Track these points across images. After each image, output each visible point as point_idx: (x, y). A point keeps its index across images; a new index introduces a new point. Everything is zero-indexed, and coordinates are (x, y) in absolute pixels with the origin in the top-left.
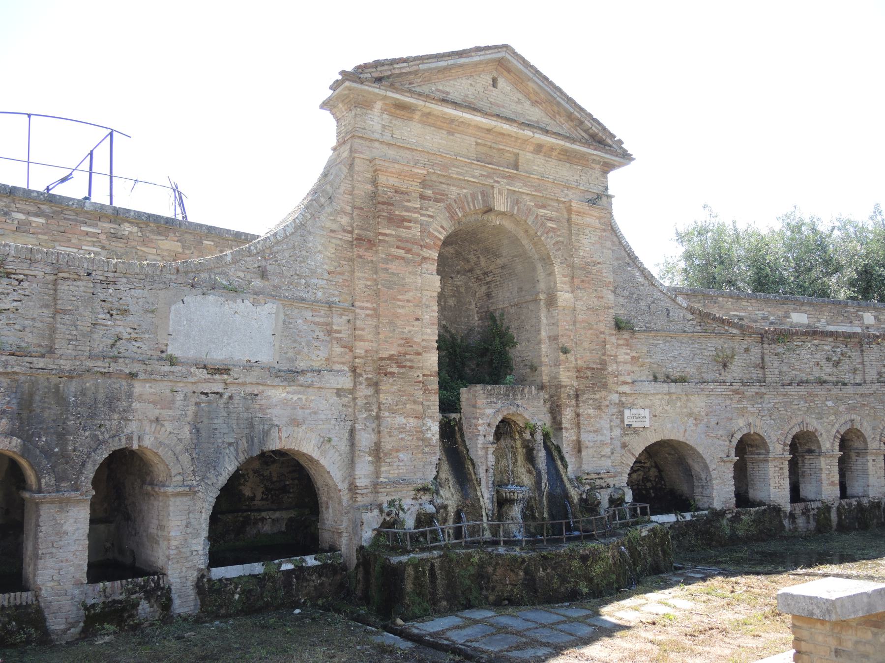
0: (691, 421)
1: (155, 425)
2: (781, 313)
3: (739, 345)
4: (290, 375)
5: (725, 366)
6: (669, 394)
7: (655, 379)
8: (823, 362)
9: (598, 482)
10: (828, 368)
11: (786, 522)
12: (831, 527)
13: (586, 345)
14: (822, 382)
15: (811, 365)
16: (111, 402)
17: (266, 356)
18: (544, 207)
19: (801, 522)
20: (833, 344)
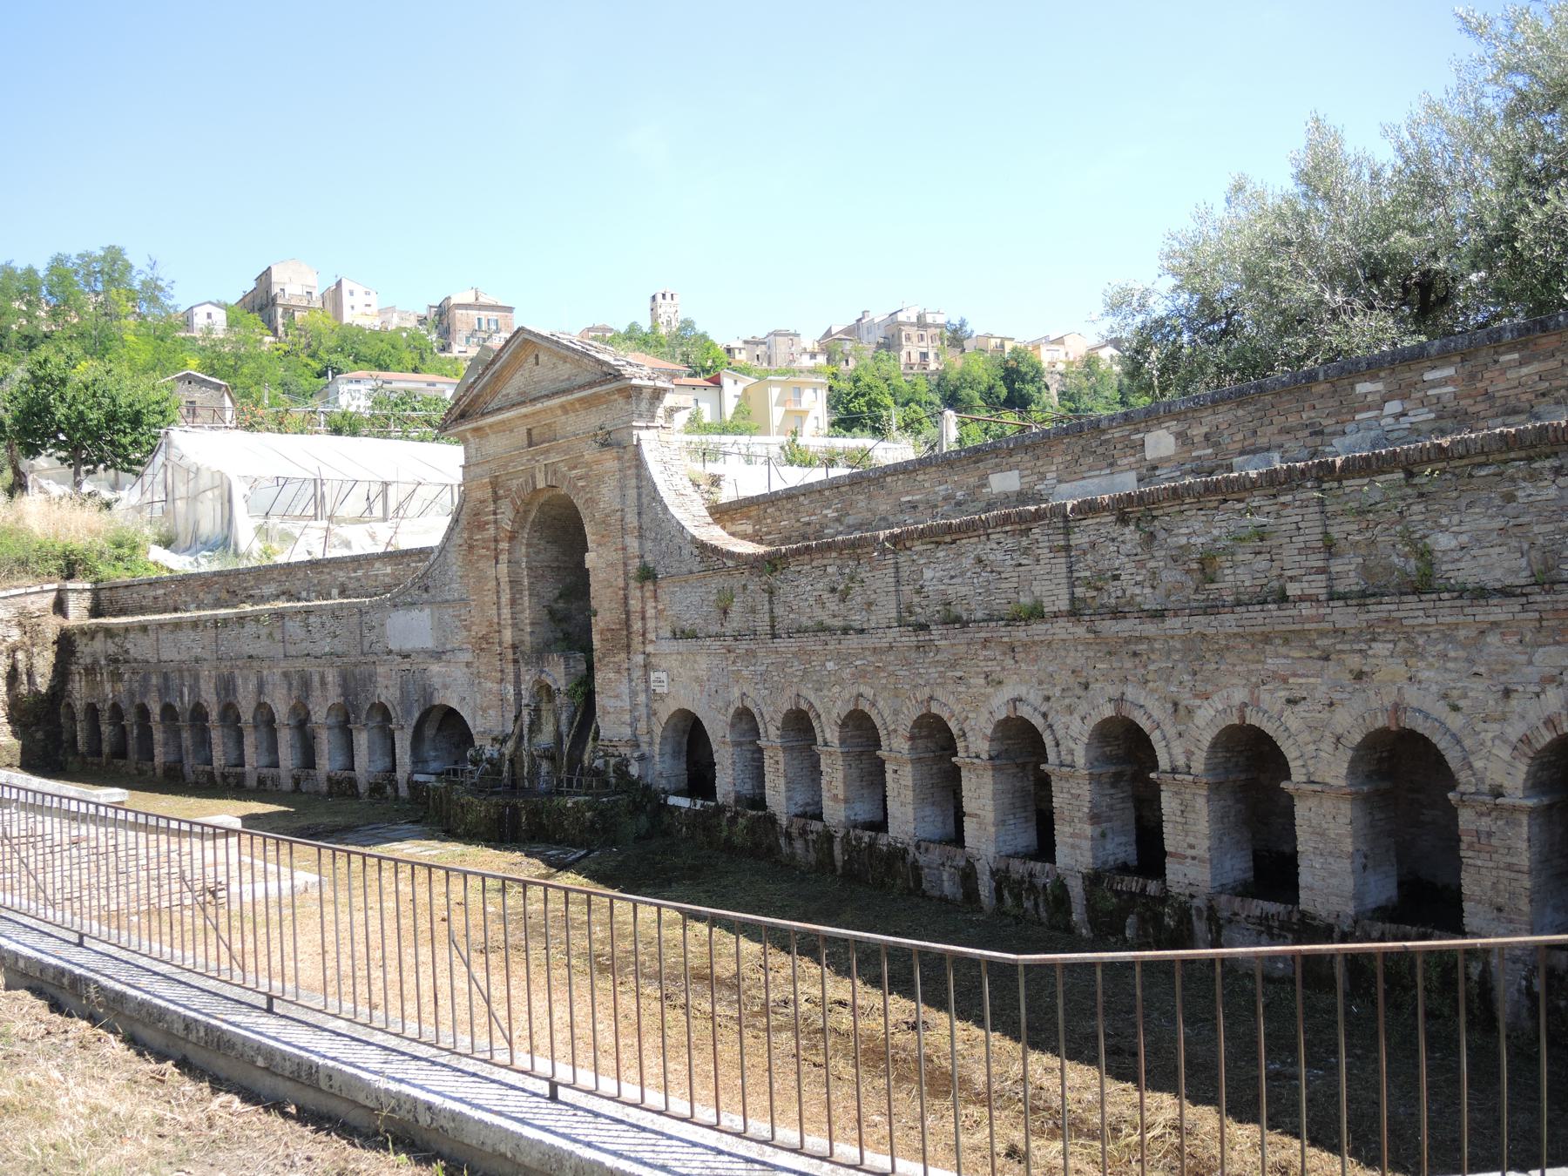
0: (697, 688)
1: (387, 691)
2: (973, 481)
3: (736, 582)
4: (437, 655)
5: (725, 612)
6: (679, 653)
7: (674, 636)
8: (826, 596)
9: (610, 750)
10: (832, 604)
11: (782, 841)
12: (834, 870)
13: (606, 605)
14: (822, 628)
15: (811, 601)
16: (371, 676)
17: (430, 644)
18: (575, 467)
19: (799, 845)
20: (839, 562)
